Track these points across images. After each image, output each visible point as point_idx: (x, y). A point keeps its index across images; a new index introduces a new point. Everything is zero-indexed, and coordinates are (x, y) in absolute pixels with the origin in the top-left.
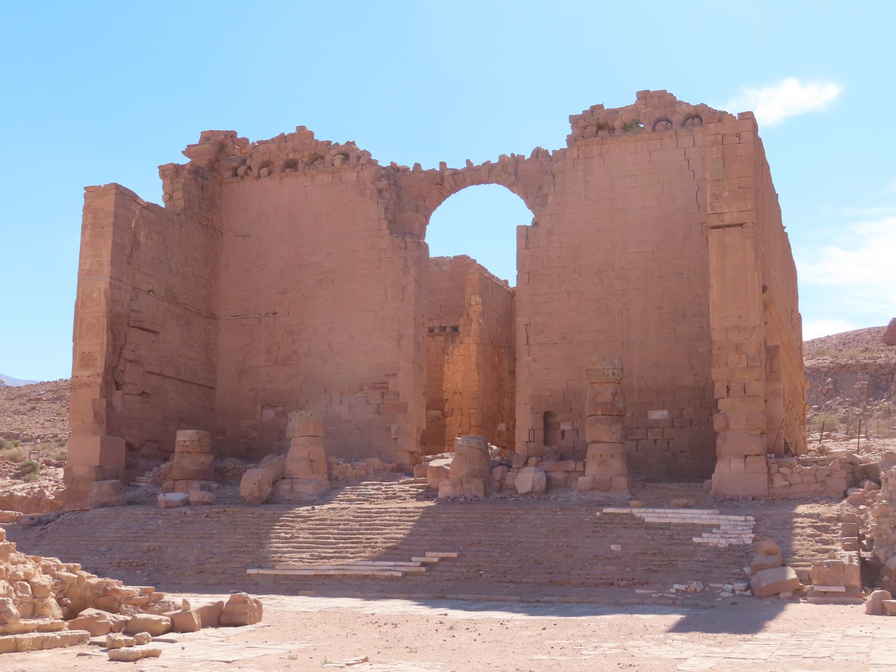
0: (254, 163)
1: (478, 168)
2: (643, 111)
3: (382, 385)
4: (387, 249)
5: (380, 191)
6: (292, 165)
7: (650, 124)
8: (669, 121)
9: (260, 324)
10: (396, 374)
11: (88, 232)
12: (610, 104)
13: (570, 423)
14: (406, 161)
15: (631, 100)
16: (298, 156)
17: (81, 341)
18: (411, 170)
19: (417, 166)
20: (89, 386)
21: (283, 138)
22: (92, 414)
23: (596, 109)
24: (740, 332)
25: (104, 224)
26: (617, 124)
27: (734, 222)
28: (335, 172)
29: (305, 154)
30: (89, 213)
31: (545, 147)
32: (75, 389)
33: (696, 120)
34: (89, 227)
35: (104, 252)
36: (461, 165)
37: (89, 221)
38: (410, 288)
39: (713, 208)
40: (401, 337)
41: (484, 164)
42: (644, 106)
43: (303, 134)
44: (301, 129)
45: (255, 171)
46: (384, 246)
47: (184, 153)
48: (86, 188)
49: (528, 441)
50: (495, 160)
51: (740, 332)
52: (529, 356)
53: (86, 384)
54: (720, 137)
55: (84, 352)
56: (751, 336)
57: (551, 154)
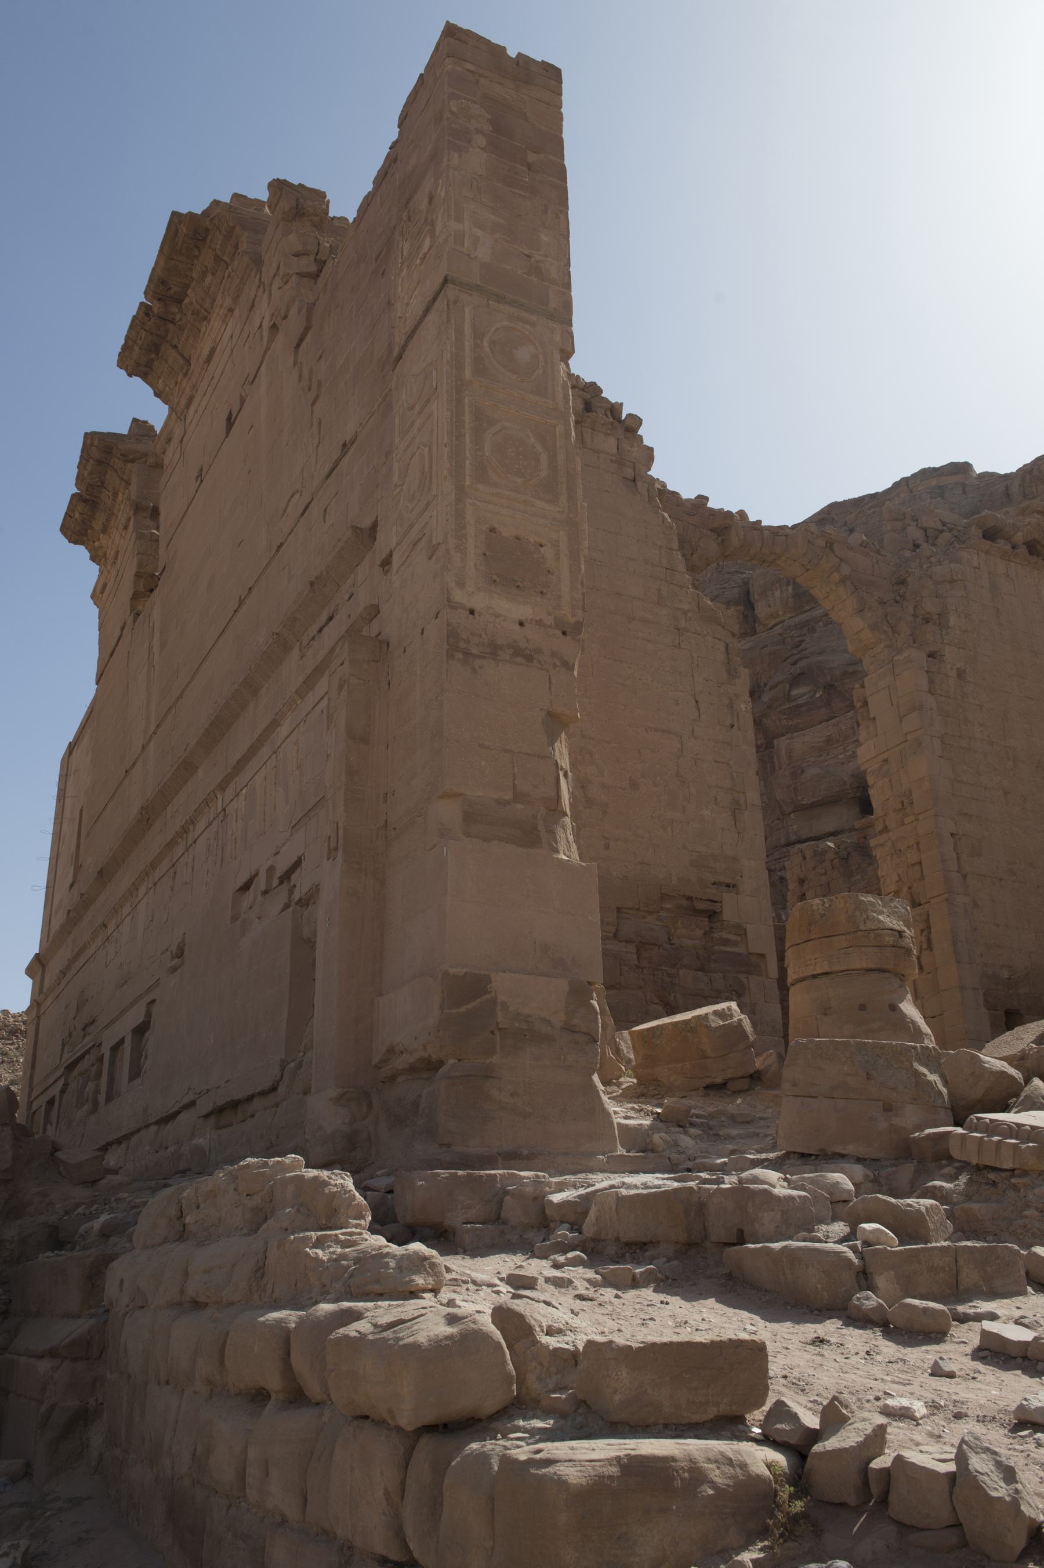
4: (689, 615)
10: (734, 886)
17: (481, 487)
20: (529, 658)
32: (467, 654)
34: (481, 141)
38: (743, 706)
46: (686, 607)
53: (518, 652)
55: (493, 530)
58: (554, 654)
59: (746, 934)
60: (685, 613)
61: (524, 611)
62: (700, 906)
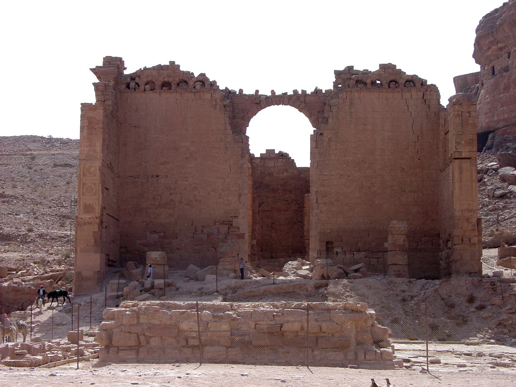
0: (142, 82)
1: (279, 96)
2: (383, 75)
3: (229, 223)
4: (230, 142)
5: (225, 106)
6: (166, 85)
7: (387, 83)
8: (396, 82)
9: (148, 182)
11: (85, 132)
12: (359, 67)
13: (341, 248)
14: (235, 87)
15: (377, 68)
16: (170, 80)
18: (237, 93)
19: (241, 91)
20: (90, 224)
21: (160, 68)
22: (93, 241)
23: (350, 69)
24: (469, 212)
25: (96, 127)
26: (369, 81)
27: (466, 157)
28: (196, 92)
29: (176, 79)
30: (85, 119)
31: (320, 88)
33: (411, 83)
34: (86, 128)
35: (97, 144)
36: (269, 94)
37: (85, 125)
38: (245, 166)
39: (456, 149)
40: (240, 195)
41: (283, 94)
42: (384, 73)
43: (173, 67)
44: (172, 63)
45: (142, 87)
46: (229, 140)
47: (91, 70)
48: (82, 104)
49: (317, 257)
50: (290, 93)
51: (469, 212)
53: (88, 223)
54: (460, 113)
55: (85, 204)
56: (474, 214)
57: (324, 92)
58: (94, 222)
59: (239, 229)
61: (90, 216)
62: (225, 223)
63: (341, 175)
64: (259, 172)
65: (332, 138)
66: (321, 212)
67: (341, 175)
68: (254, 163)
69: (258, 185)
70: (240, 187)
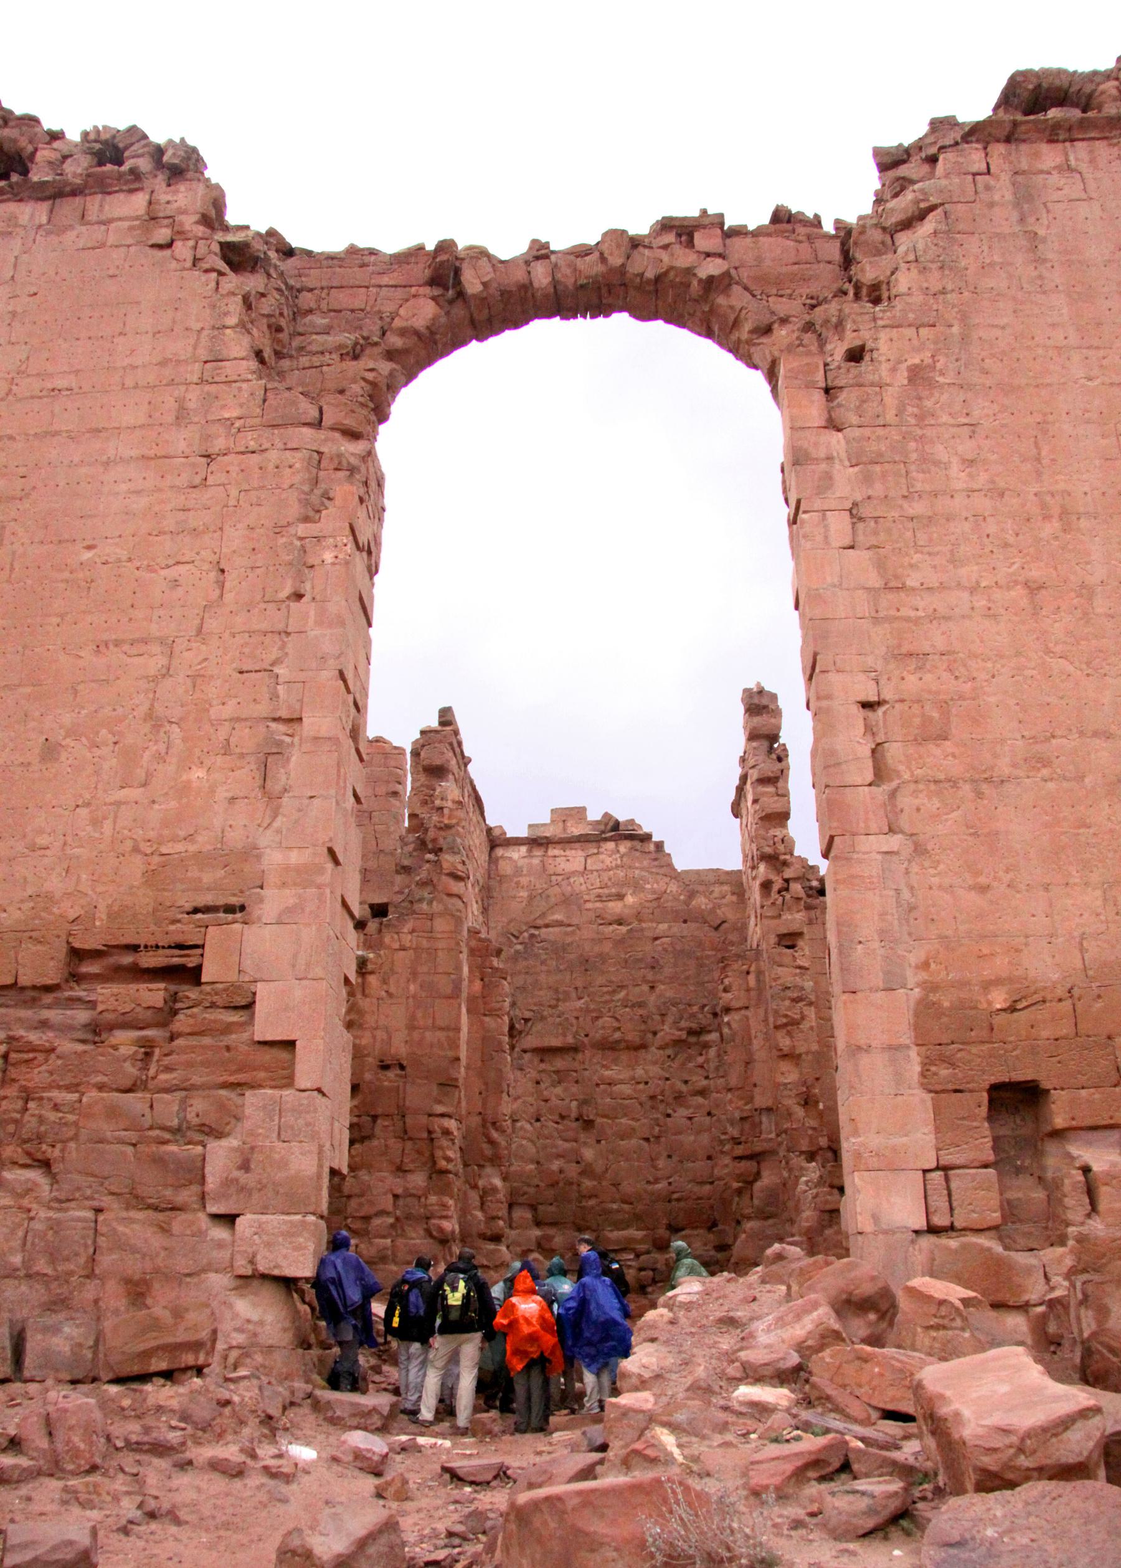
10: (242, 908)
38: (328, 557)
52: (892, 830)
60: (230, 422)
62: (149, 960)
63: (1033, 588)
64: (524, 894)
65: (933, 367)
66: (920, 850)
67: (1033, 588)
68: (501, 863)
69: (519, 947)
70: (274, 696)
